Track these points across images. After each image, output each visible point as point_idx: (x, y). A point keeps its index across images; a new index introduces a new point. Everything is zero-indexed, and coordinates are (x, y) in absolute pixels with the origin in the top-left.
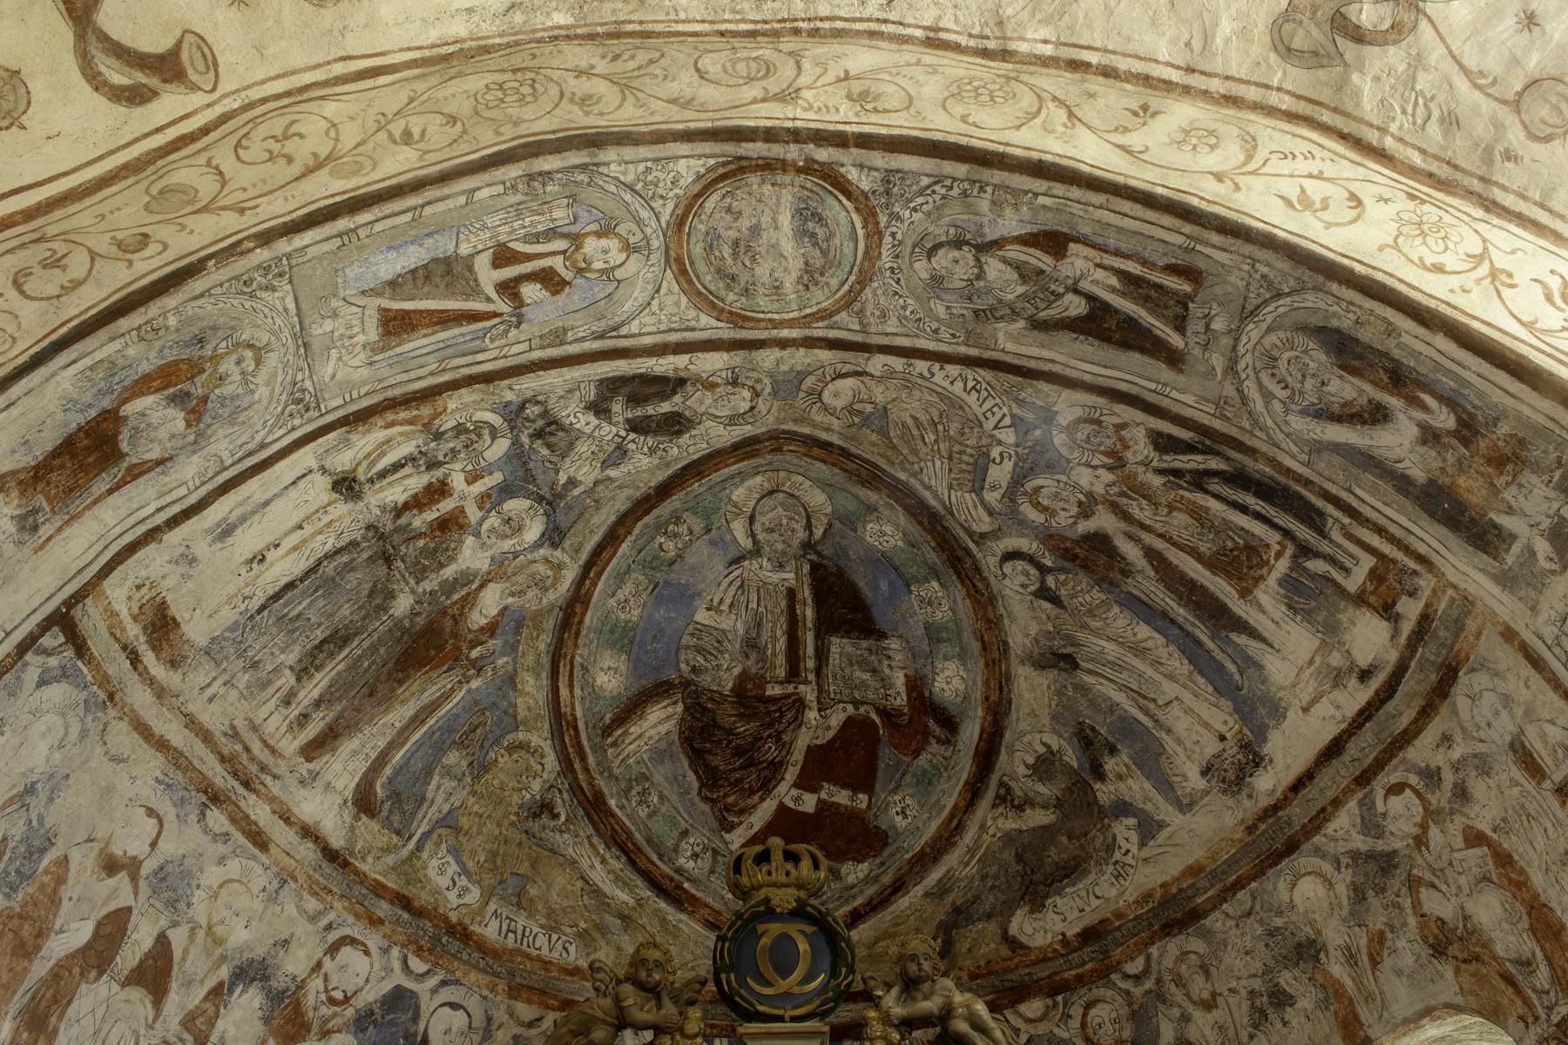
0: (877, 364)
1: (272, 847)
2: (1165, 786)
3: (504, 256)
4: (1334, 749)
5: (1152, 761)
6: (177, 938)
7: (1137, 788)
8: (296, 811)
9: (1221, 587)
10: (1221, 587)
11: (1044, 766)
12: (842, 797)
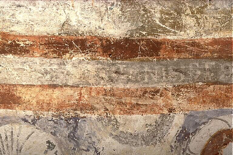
1: (21, 92)
8: (18, 29)
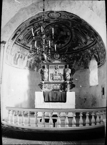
0: (62, 20)
2: (82, 43)
3: (37, 18)
4: (91, 44)
5: (81, 41)
6: (22, 55)
7: (80, 42)
9: (85, 34)
10: (85, 34)
11: (75, 40)
12: (62, 40)
